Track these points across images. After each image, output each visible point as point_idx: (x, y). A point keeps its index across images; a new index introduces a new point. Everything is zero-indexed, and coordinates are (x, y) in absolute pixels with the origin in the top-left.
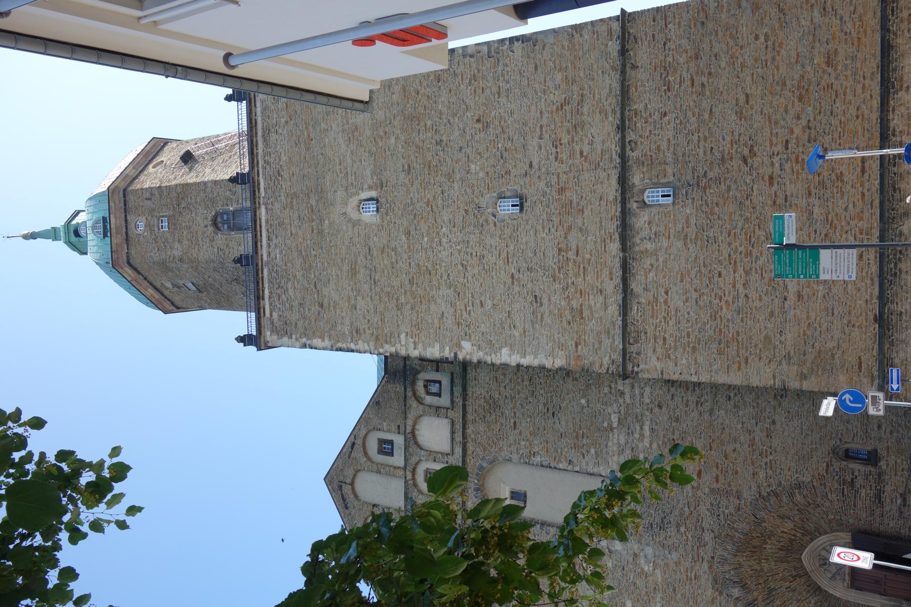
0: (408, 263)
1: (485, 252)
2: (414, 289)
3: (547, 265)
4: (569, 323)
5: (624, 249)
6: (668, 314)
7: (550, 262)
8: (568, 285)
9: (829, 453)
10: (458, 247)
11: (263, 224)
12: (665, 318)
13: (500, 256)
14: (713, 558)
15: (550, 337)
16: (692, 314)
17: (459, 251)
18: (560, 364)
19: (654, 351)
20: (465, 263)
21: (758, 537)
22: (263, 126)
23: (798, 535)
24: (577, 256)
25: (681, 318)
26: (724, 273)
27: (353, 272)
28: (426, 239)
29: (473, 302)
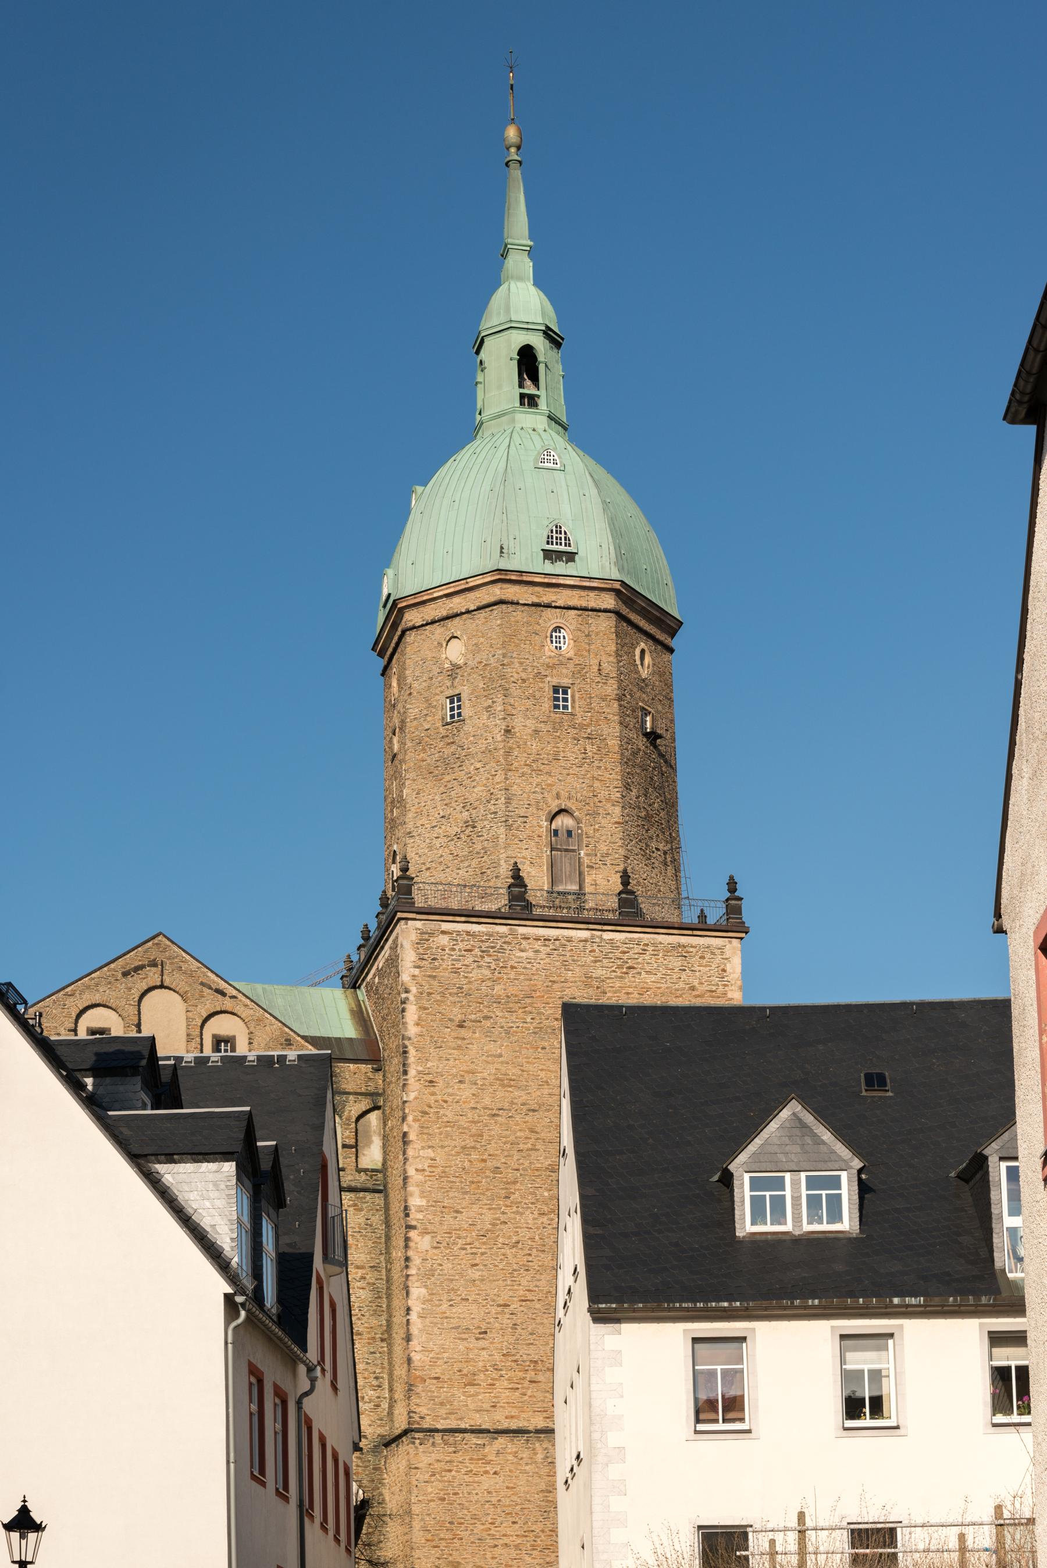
0: (516, 1167)
1: (532, 1272)
2: (488, 1173)
3: (520, 1347)
4: (460, 1371)
5: (538, 1431)
6: (475, 1474)
7: (523, 1350)
8: (501, 1370)
10: (537, 1238)
11: (566, 932)
12: (471, 1471)
13: (529, 1290)
15: (443, 1348)
16: (476, 1497)
17: (532, 1239)
18: (414, 1358)
19: (438, 1461)
20: (520, 1245)
22: (692, 947)
24: (530, 1381)
25: (472, 1487)
26: (517, 1526)
27: (505, 1082)
28: (546, 1194)
29: (476, 1254)
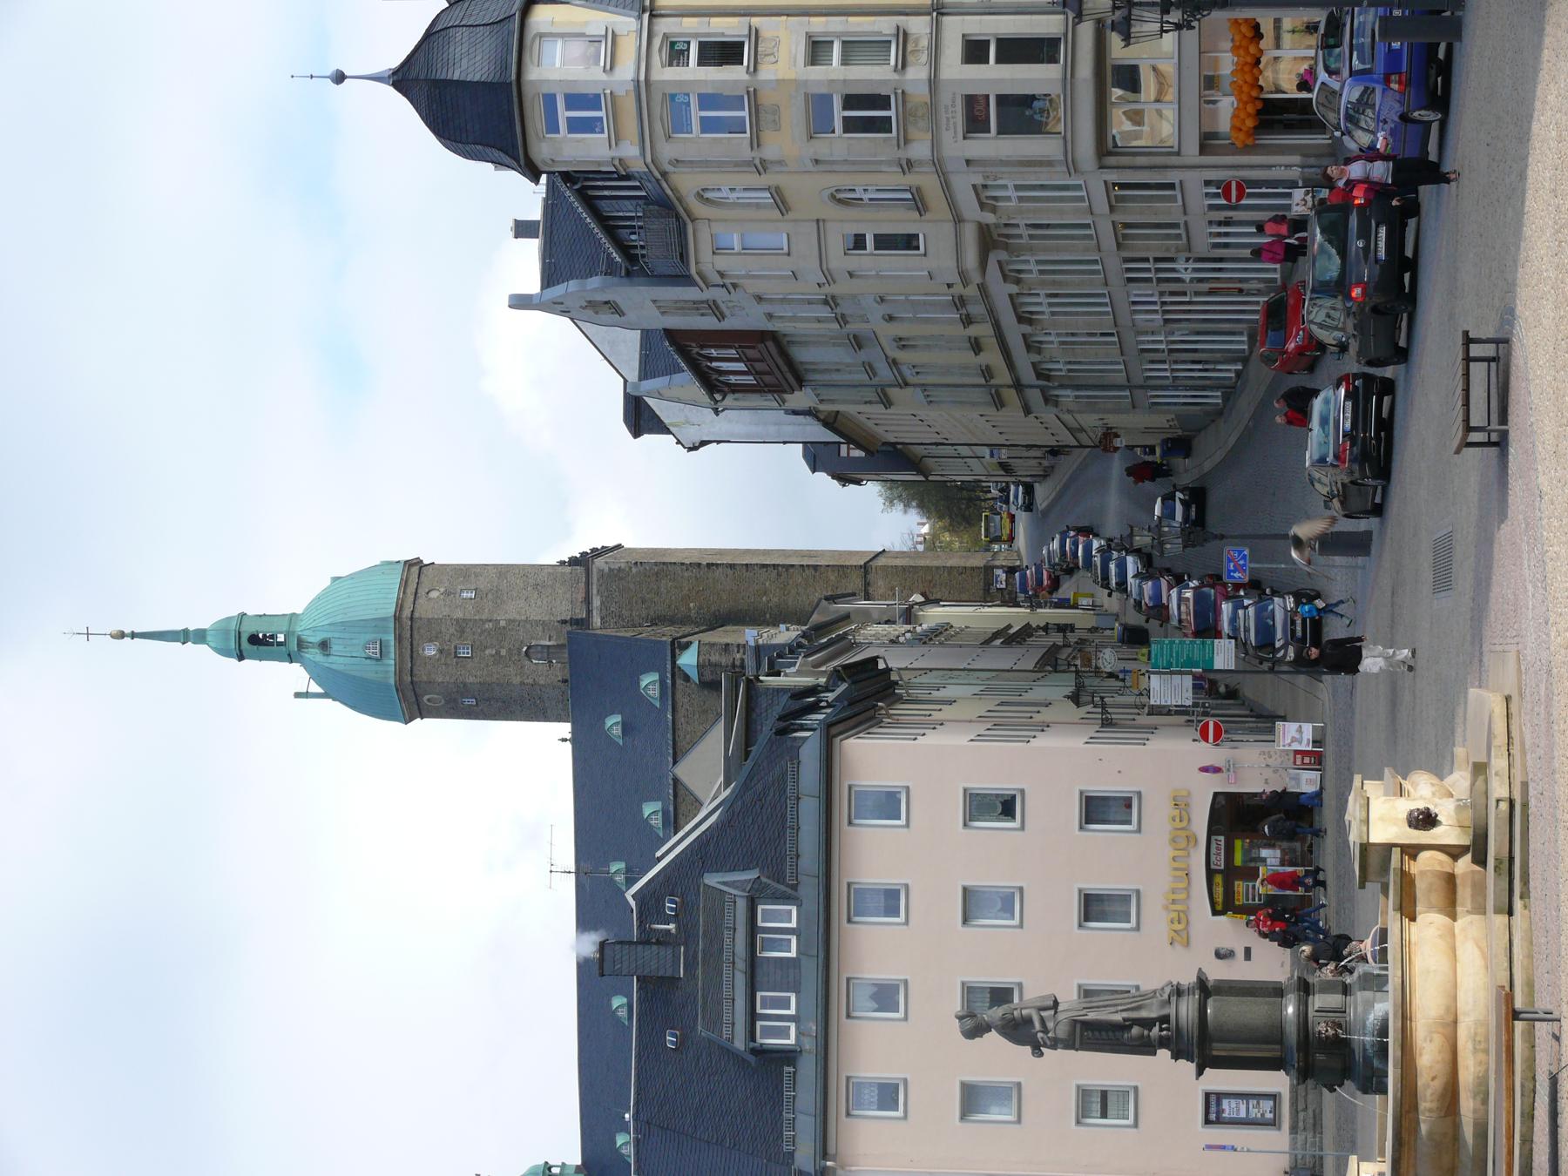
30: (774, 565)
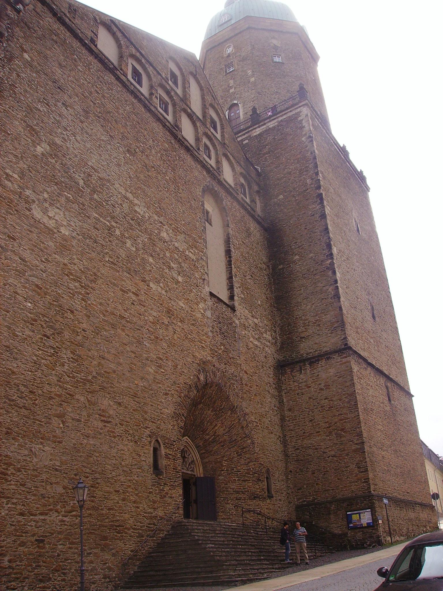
9: (267, 467)
14: (214, 366)
21: (221, 406)
23: (208, 437)
30: (332, 254)
